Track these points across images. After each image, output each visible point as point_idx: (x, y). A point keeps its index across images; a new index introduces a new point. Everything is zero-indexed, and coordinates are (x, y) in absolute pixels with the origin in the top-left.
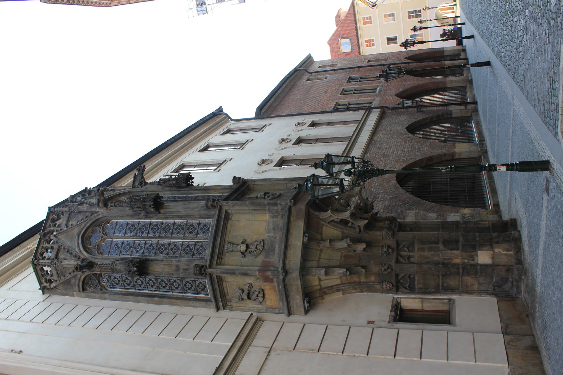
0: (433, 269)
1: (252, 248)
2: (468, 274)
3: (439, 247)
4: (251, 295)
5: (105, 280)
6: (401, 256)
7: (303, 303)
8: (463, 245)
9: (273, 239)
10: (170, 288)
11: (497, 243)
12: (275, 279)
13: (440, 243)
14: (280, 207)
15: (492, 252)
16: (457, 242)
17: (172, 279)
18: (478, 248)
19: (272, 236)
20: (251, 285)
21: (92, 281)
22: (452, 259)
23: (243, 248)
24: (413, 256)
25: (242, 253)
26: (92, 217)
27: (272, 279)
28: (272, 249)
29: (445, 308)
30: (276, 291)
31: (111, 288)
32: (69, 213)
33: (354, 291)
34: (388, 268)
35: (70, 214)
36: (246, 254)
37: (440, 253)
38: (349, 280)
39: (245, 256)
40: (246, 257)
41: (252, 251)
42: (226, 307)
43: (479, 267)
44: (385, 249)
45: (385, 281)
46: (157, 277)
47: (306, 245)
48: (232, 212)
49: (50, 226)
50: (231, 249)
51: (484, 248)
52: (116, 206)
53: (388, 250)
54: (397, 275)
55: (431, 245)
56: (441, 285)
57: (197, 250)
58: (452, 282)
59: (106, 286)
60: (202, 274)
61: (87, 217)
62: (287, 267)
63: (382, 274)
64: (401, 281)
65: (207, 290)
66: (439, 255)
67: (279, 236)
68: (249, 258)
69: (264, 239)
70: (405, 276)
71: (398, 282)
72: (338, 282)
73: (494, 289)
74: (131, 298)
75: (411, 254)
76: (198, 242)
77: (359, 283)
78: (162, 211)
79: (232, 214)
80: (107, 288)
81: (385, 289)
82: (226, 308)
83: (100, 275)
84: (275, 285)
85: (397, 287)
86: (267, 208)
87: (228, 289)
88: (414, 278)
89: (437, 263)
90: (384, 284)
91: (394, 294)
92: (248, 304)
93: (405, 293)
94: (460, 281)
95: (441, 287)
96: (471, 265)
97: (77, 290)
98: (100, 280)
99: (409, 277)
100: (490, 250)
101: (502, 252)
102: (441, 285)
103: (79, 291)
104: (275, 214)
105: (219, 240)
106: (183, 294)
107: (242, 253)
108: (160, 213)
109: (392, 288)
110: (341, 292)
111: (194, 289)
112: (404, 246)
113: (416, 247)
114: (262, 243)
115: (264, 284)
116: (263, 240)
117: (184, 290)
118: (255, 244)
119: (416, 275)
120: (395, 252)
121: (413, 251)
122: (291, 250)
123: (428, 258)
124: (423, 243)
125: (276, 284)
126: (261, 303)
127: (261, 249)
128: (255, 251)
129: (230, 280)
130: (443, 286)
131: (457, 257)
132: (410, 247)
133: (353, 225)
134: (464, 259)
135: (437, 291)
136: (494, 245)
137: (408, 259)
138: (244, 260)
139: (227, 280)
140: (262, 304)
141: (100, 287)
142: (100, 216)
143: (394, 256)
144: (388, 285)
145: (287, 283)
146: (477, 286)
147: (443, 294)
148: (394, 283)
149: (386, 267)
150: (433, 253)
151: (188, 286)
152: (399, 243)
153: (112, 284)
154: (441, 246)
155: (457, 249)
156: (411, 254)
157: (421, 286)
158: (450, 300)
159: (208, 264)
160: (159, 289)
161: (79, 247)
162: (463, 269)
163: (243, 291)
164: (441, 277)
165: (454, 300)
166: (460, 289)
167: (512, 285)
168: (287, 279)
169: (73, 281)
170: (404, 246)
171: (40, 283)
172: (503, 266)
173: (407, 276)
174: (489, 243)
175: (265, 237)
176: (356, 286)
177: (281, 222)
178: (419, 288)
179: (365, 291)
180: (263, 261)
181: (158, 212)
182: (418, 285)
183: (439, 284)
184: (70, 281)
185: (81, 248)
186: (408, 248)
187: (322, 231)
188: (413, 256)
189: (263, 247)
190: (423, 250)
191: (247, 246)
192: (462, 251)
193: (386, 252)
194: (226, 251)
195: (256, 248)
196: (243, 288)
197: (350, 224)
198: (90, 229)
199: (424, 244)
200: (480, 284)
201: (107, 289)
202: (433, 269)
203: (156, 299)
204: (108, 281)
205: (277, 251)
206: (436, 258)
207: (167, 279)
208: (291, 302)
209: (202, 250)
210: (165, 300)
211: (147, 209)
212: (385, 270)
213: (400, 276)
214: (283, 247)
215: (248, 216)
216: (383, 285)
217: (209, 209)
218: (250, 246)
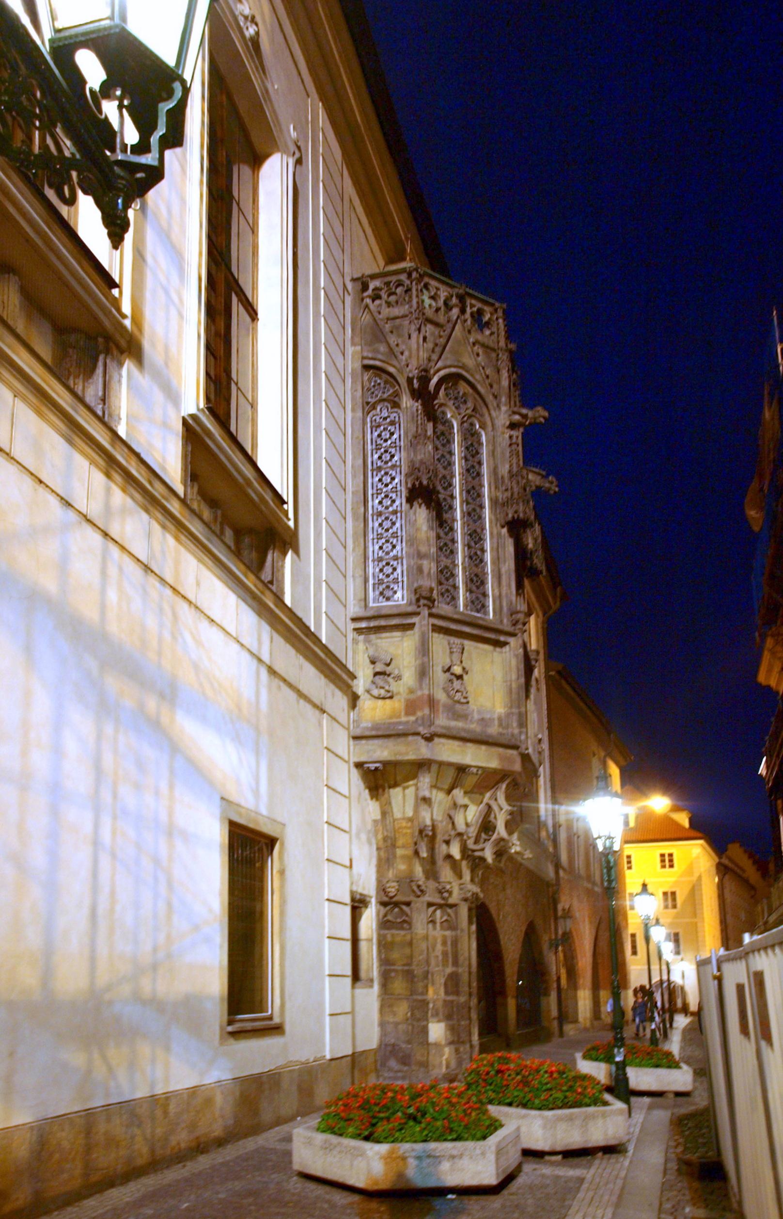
0: (421, 957)
1: (457, 684)
2: (412, 1009)
3: (448, 967)
4: (382, 677)
5: (385, 413)
6: (435, 911)
7: (375, 760)
8: (452, 1002)
9: (470, 718)
10: (380, 537)
11: (457, 1051)
12: (412, 718)
13: (454, 969)
14: (516, 731)
15: (443, 1042)
16: (457, 993)
17: (397, 540)
18: (451, 1023)
19: (472, 717)
20: (398, 678)
21: (382, 385)
22: (433, 984)
23: (457, 670)
24: (435, 929)
25: (449, 669)
26: (491, 397)
27: (413, 714)
28: (457, 716)
29: (363, 974)
30: (391, 718)
31: (371, 422)
32: (496, 348)
33: (380, 836)
34: (422, 891)
35: (493, 350)
36: (448, 674)
37: (440, 968)
38: (400, 830)
39: (445, 672)
40: (442, 673)
41: (452, 683)
42: (357, 633)
43: (425, 1023)
44: (448, 887)
45: (399, 886)
46: (399, 514)
47: (465, 769)
48: (506, 652)
49: (472, 306)
50: (455, 650)
51: (448, 1033)
52: (510, 445)
53: (447, 891)
54: (408, 904)
55: (450, 955)
56: (392, 967)
57: (448, 591)
58: (399, 986)
59: (374, 412)
60: (418, 600)
61: (491, 386)
62: (436, 740)
63: (412, 881)
64: (396, 910)
65: (382, 602)
66: (437, 966)
67: (474, 727)
68: (440, 677)
69: (470, 703)
70: (407, 915)
71: (396, 904)
72: (398, 814)
73: (389, 1045)
74: (360, 461)
75: (438, 925)
76: (458, 593)
77: (394, 846)
78: (505, 531)
79: (501, 652)
80: (371, 414)
81: (388, 885)
82: (355, 633)
83: (396, 405)
84: (400, 718)
85: (387, 903)
86: (515, 711)
87: (389, 640)
88: (402, 929)
89: (428, 963)
90: (395, 884)
91: (377, 898)
92: (364, 670)
93: (378, 914)
94: (400, 997)
95: (388, 968)
96: (427, 1012)
97: (365, 354)
98: (386, 404)
99: (404, 921)
100: (446, 1039)
101: (445, 1057)
102: (392, 967)
103: (363, 358)
104: (504, 722)
105: (467, 629)
106: (371, 559)
107: (449, 669)
108: (503, 527)
109: (387, 896)
110: (379, 817)
111: (382, 580)
112: (449, 915)
113: (448, 933)
114: (464, 701)
115: (403, 700)
116: (468, 703)
117: (379, 561)
118: (462, 689)
119: (409, 931)
120: (442, 902)
121: (442, 928)
122: (459, 746)
123: (434, 950)
124: (455, 943)
125: (404, 719)
126: (368, 691)
127: (456, 698)
128: (453, 689)
129: (405, 644)
130: (390, 971)
131: (436, 993)
132: (450, 925)
133: (482, 840)
134: (434, 1002)
135: (385, 962)
136: (453, 1047)
137: (431, 921)
138: (438, 670)
139: (405, 639)
140: (366, 694)
141: (373, 400)
142: (492, 412)
143: (438, 900)
144: (393, 890)
145: (410, 738)
146: (391, 1020)
147: (380, 971)
148: (394, 899)
149: (423, 888)
150: (440, 958)
151: (387, 570)
152: (454, 908)
153: (379, 426)
154: (449, 970)
155: (447, 993)
156: (438, 925)
157: (389, 938)
158: (372, 980)
159: (434, 611)
160: (377, 516)
161: (445, 367)
162: (424, 1001)
163: (388, 665)
164: (406, 968)
165: (371, 986)
166: (387, 997)
167: (397, 1072)
168: (419, 738)
169: (382, 348)
170: (449, 915)
171: (373, 277)
172: (427, 1059)
173: (407, 919)
174: (456, 1039)
175: (472, 706)
176: (389, 841)
177: (494, 730)
178: (385, 936)
179: (379, 855)
180: (438, 701)
181: (503, 522)
182: (389, 934)
183: (394, 964)
184: (381, 342)
185: (442, 373)
186: (446, 920)
187: (476, 793)
188: (435, 929)
189: (459, 702)
190: (444, 943)
191: (460, 677)
192: (445, 1001)
193: (444, 888)
194: (452, 642)
195: (457, 691)
196: (392, 665)
197: (483, 836)
198: (471, 391)
199: (452, 944)
200: (396, 1024)
201: (368, 413)
202: (421, 957)
203: (362, 510)
204: (385, 419)
205: (453, 724)
206: (433, 962)
207: (397, 533)
208: (376, 742)
209: (448, 600)
210: (362, 525)
211: (512, 506)
212: (419, 886)
213: (404, 907)
214: (463, 734)
215: (499, 677)
216: (393, 881)
217: (511, 615)
218: (459, 681)
